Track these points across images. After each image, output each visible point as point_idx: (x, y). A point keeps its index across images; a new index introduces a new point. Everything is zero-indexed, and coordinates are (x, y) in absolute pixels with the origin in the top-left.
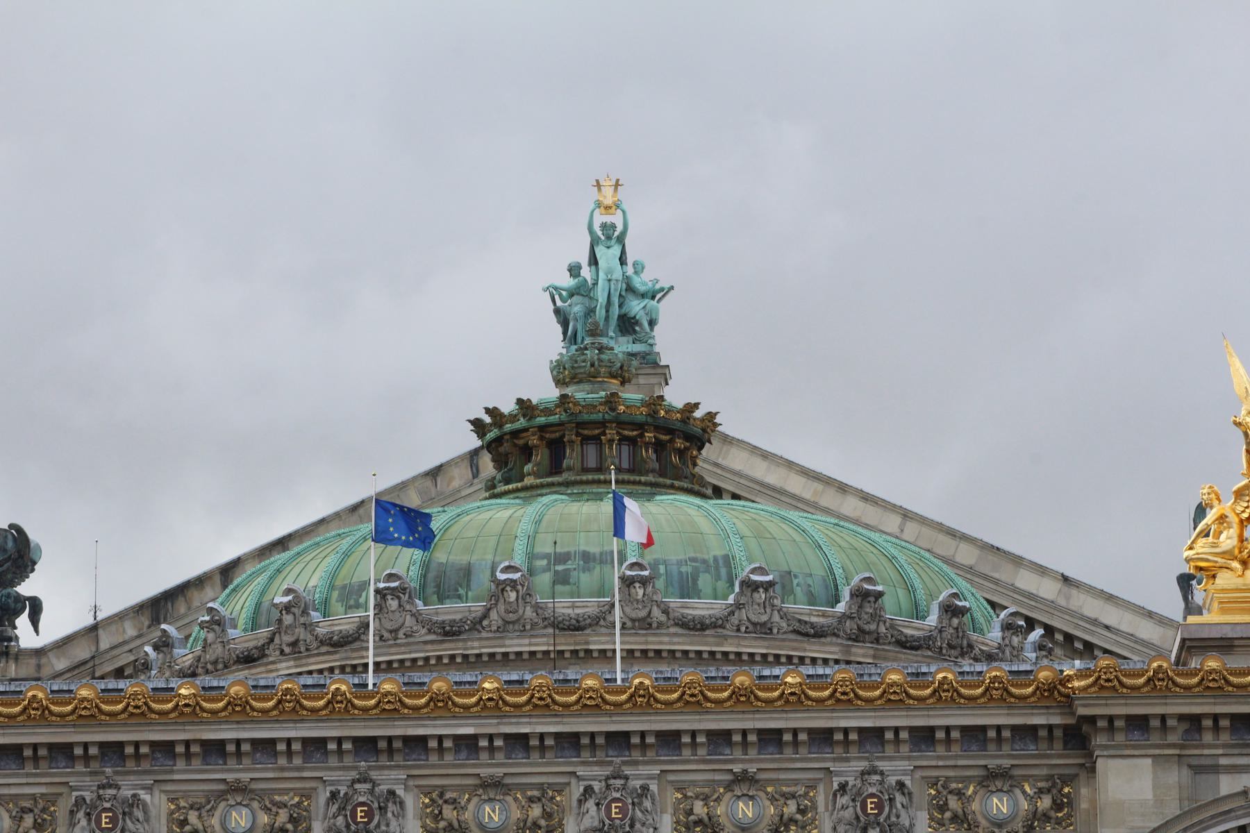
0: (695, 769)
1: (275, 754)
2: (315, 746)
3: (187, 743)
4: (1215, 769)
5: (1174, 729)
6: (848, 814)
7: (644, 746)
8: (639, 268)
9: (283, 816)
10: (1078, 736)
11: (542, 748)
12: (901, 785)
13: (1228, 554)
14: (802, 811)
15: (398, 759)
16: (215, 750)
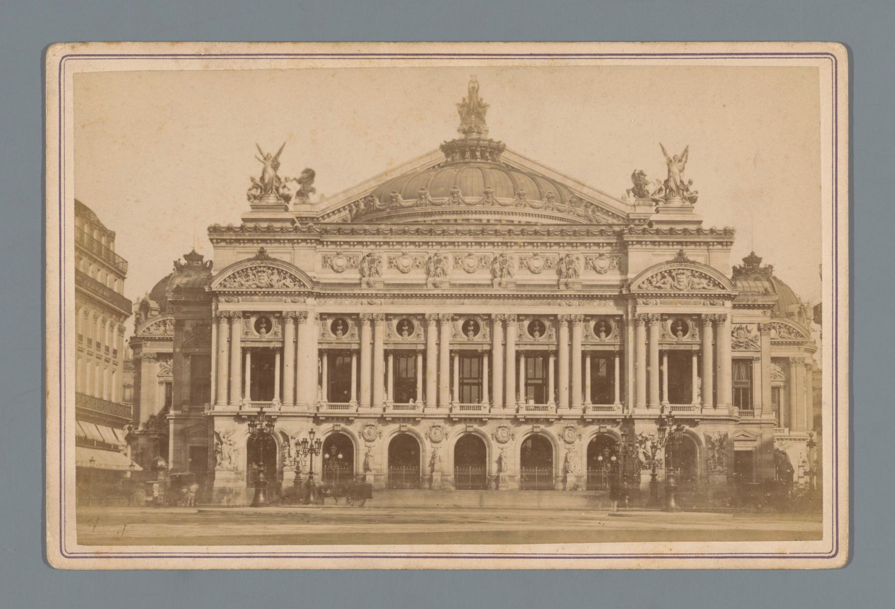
8: (482, 100)
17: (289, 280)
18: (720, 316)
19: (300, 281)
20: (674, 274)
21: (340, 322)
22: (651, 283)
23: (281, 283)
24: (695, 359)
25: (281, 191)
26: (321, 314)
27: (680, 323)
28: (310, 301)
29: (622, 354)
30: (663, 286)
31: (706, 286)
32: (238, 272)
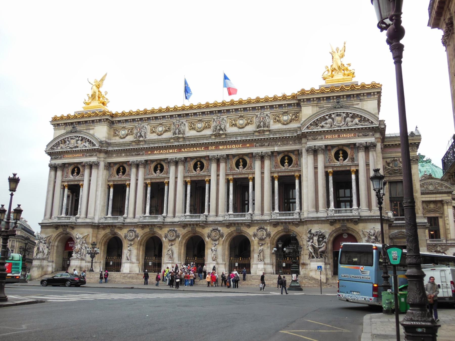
0: (233, 115)
1: (166, 118)
2: (171, 116)
3: (152, 117)
4: (324, 107)
5: (315, 100)
6: (258, 120)
7: (224, 112)
9: (167, 128)
10: (298, 105)
11: (208, 114)
12: (267, 115)
13: (329, 76)
14: (251, 121)
15: (185, 118)
16: (156, 118)
17: (87, 143)
18: (372, 143)
19: (93, 143)
20: (333, 116)
21: (122, 168)
22: (317, 125)
23: (82, 145)
24: (353, 177)
25: (101, 99)
26: (110, 163)
27: (341, 152)
28: (102, 155)
29: (300, 177)
30: (325, 125)
31: (357, 122)
32: (61, 140)
